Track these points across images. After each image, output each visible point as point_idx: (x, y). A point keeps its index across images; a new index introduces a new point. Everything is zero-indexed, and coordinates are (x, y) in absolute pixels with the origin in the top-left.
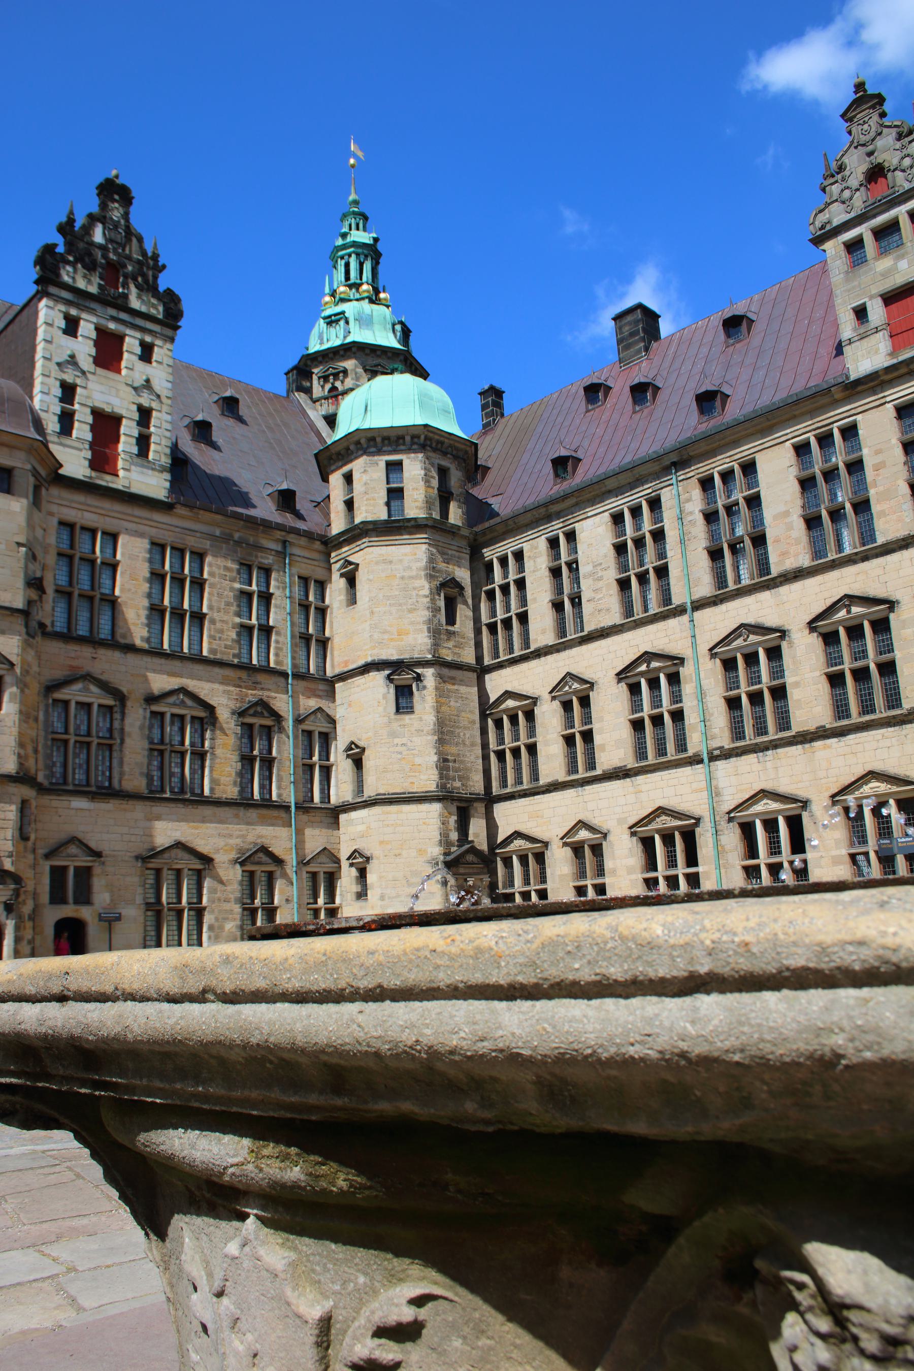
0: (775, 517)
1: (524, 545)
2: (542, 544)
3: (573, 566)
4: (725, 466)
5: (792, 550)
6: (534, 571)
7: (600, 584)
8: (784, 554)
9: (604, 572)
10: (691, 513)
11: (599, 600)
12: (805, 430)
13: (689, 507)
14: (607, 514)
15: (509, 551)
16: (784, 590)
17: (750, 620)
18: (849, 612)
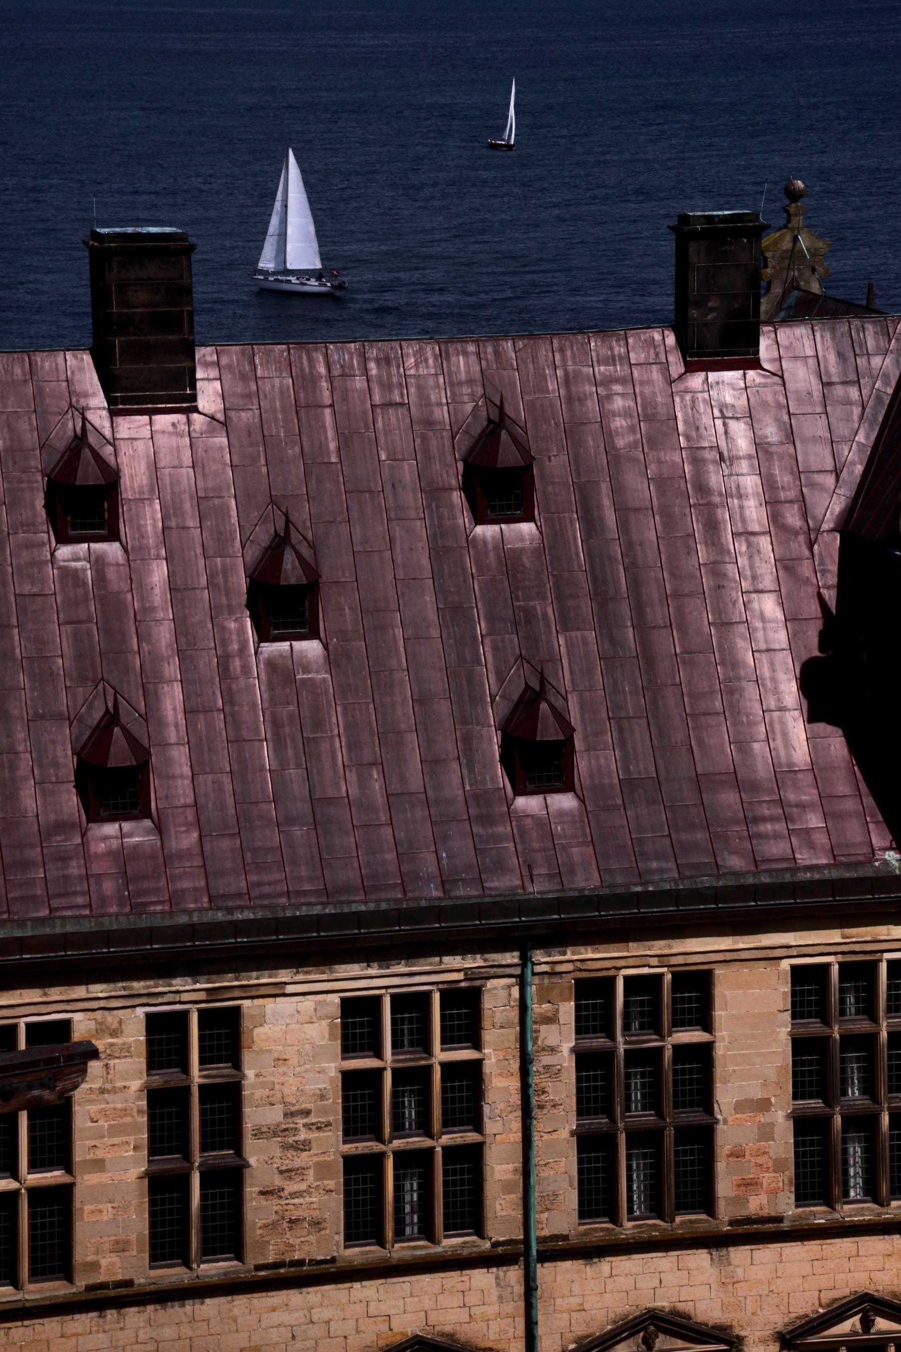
0: (740, 1107)
1: (77, 1017)
2: (133, 1028)
3: (226, 1100)
4: (646, 971)
5: (767, 1178)
6: (102, 1091)
7: (302, 1159)
8: (750, 1185)
9: (314, 1135)
10: (553, 1050)
11: (293, 1195)
12: (823, 944)
13: (548, 1035)
14: (336, 999)
15: (22, 1023)
16: (739, 1254)
17: (663, 1303)
18: (867, 1324)
